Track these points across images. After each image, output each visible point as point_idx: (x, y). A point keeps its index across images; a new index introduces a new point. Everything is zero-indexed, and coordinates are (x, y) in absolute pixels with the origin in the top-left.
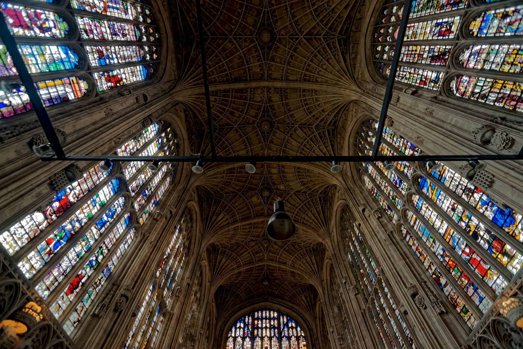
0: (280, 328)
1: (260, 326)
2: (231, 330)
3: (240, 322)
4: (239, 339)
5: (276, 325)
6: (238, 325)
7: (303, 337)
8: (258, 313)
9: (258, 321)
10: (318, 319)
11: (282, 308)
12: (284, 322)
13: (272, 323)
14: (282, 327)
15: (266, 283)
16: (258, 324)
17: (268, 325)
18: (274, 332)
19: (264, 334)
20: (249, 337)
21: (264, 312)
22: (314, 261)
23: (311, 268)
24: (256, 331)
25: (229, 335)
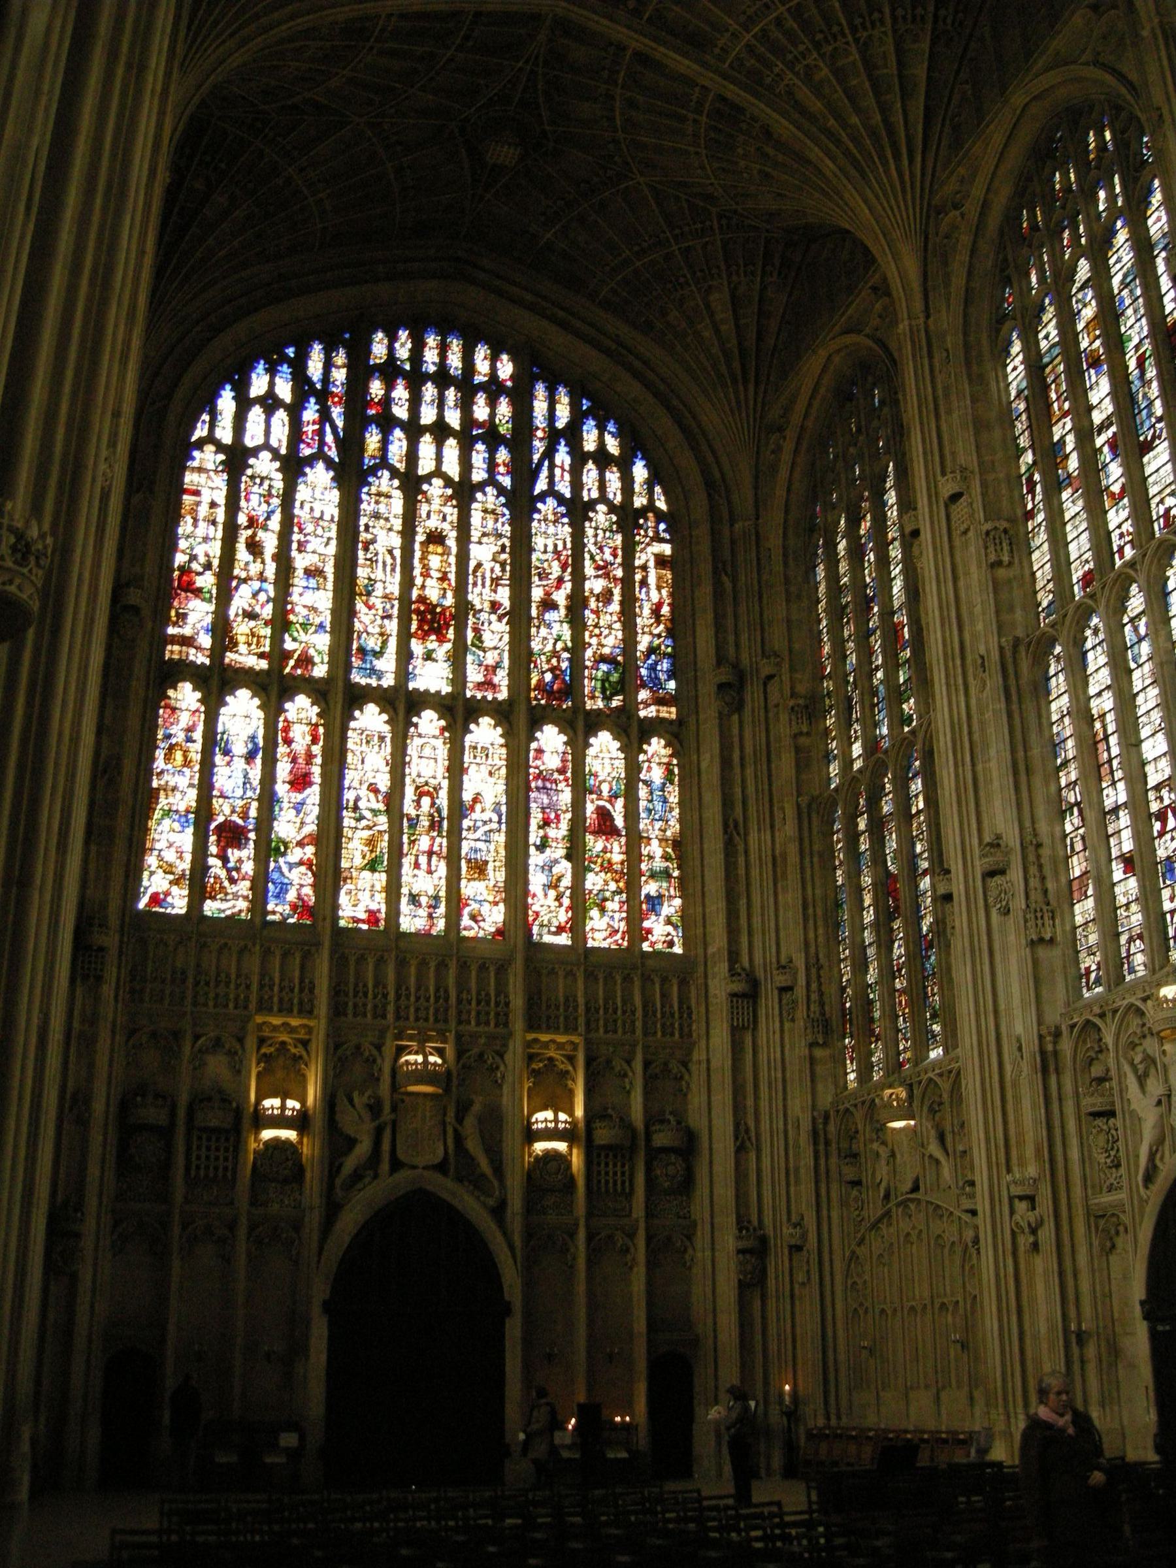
0: (530, 450)
1: (401, 412)
2: (210, 405)
3: (272, 371)
4: (264, 464)
5: (504, 429)
6: (259, 384)
7: (660, 516)
8: (392, 338)
9: (390, 386)
10: (791, 434)
11: (558, 340)
12: (551, 416)
13: (481, 412)
14: (539, 446)
15: (504, 153)
16: (387, 401)
17: (453, 418)
18: (492, 465)
19: (426, 465)
20: (329, 464)
21: (432, 340)
22: (920, 71)
23: (884, 109)
24: (373, 439)
25: (200, 432)
